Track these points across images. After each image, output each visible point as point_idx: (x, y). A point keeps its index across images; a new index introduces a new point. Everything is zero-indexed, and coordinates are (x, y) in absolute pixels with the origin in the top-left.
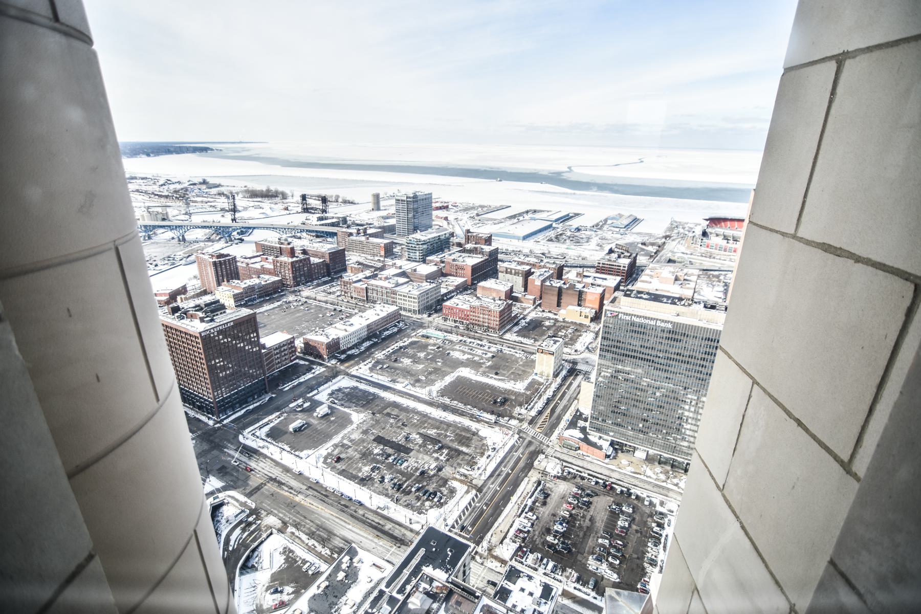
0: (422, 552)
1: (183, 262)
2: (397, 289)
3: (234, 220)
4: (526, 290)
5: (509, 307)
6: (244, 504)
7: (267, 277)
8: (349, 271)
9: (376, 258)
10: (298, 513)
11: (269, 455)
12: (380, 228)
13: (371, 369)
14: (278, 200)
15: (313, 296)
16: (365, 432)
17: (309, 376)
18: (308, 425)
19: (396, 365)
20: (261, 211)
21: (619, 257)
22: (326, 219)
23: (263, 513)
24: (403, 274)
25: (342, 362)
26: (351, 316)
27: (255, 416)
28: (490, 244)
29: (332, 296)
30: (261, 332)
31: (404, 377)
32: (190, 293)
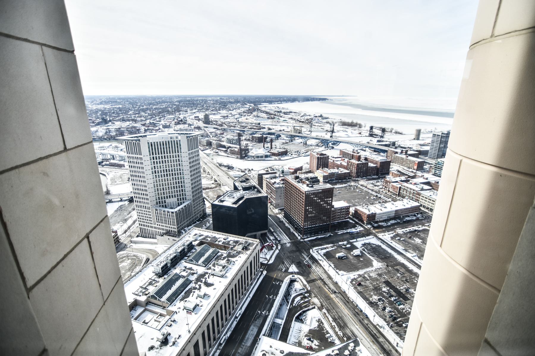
1: (303, 155)
2: (421, 192)
3: (331, 137)
6: (305, 286)
7: (342, 169)
8: (391, 175)
9: (411, 170)
10: (330, 304)
11: (323, 265)
12: (417, 151)
13: (392, 238)
14: (356, 128)
15: (365, 185)
16: (380, 275)
17: (353, 230)
18: (347, 258)
19: (410, 241)
20: (346, 133)
22: (382, 141)
23: (313, 295)
24: (428, 183)
25: (375, 228)
26: (386, 202)
27: (320, 242)
29: (377, 188)
30: (334, 198)
31: (414, 250)
32: (304, 171)
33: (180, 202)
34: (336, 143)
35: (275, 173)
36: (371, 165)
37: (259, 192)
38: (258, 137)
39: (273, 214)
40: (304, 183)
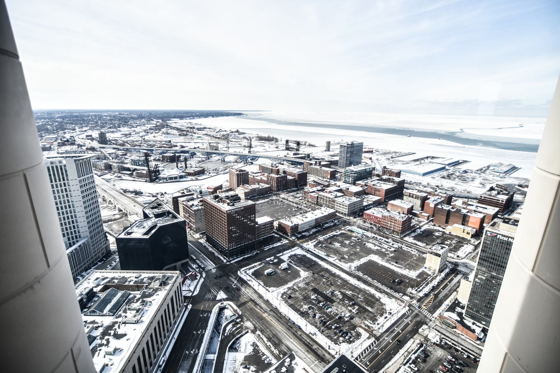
1: (222, 172)
2: (336, 199)
3: (249, 152)
4: (422, 209)
5: (409, 220)
6: (235, 311)
7: (263, 184)
8: (308, 186)
9: (325, 180)
10: (264, 324)
11: (252, 286)
12: (328, 161)
13: (315, 246)
14: (273, 142)
15: (286, 198)
16: (307, 284)
17: (279, 244)
18: (275, 273)
19: (331, 246)
20: (264, 148)
22: (298, 154)
23: (245, 319)
24: (340, 191)
25: (299, 239)
26: (306, 212)
27: (248, 262)
28: (399, 177)
29: (297, 199)
30: (257, 215)
31: (335, 254)
32: (224, 189)
33: (71, 241)
34: (255, 158)
35: (193, 194)
36: (290, 177)
37: (175, 217)
38: (170, 157)
39: (194, 240)
40: (224, 202)
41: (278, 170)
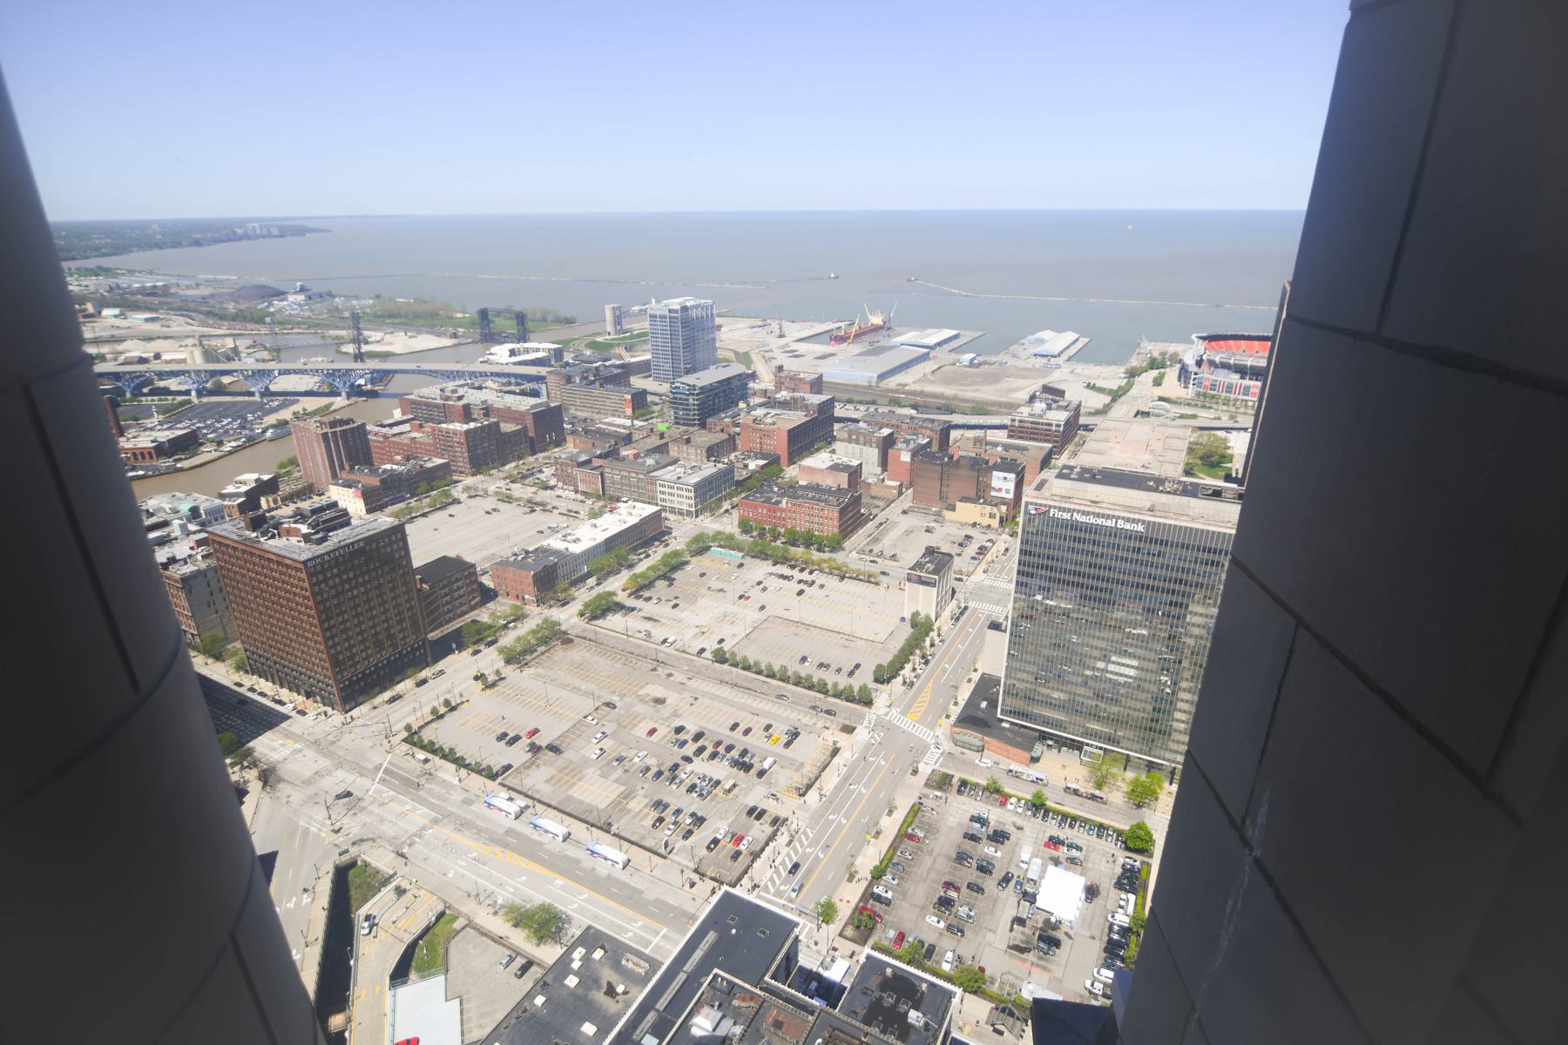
0: (711, 936)
21: (1049, 408)
22: (527, 351)
35: (165, 524)
36: (508, 427)
40: (289, 532)
41: (467, 408)
